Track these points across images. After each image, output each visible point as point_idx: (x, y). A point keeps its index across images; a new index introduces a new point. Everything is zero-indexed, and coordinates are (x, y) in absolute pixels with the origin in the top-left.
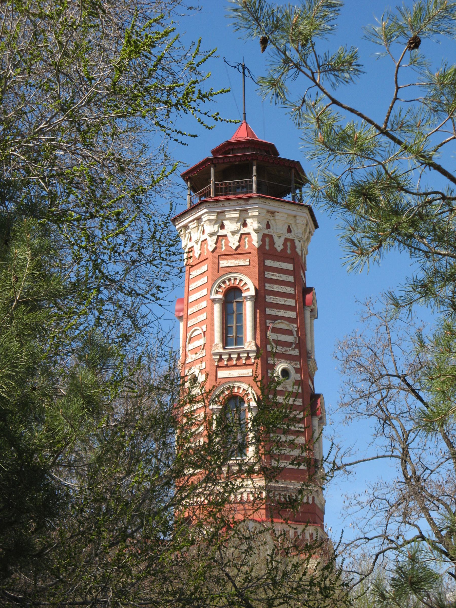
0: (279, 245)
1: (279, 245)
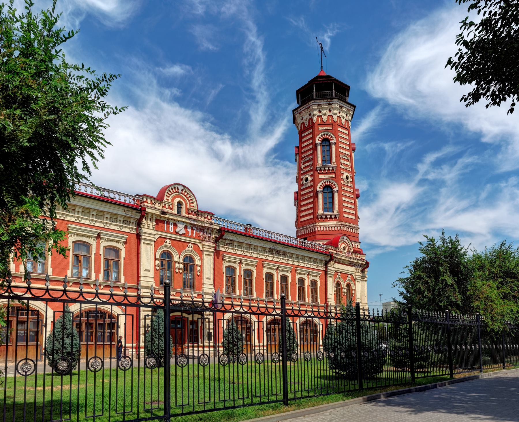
1: (343, 121)
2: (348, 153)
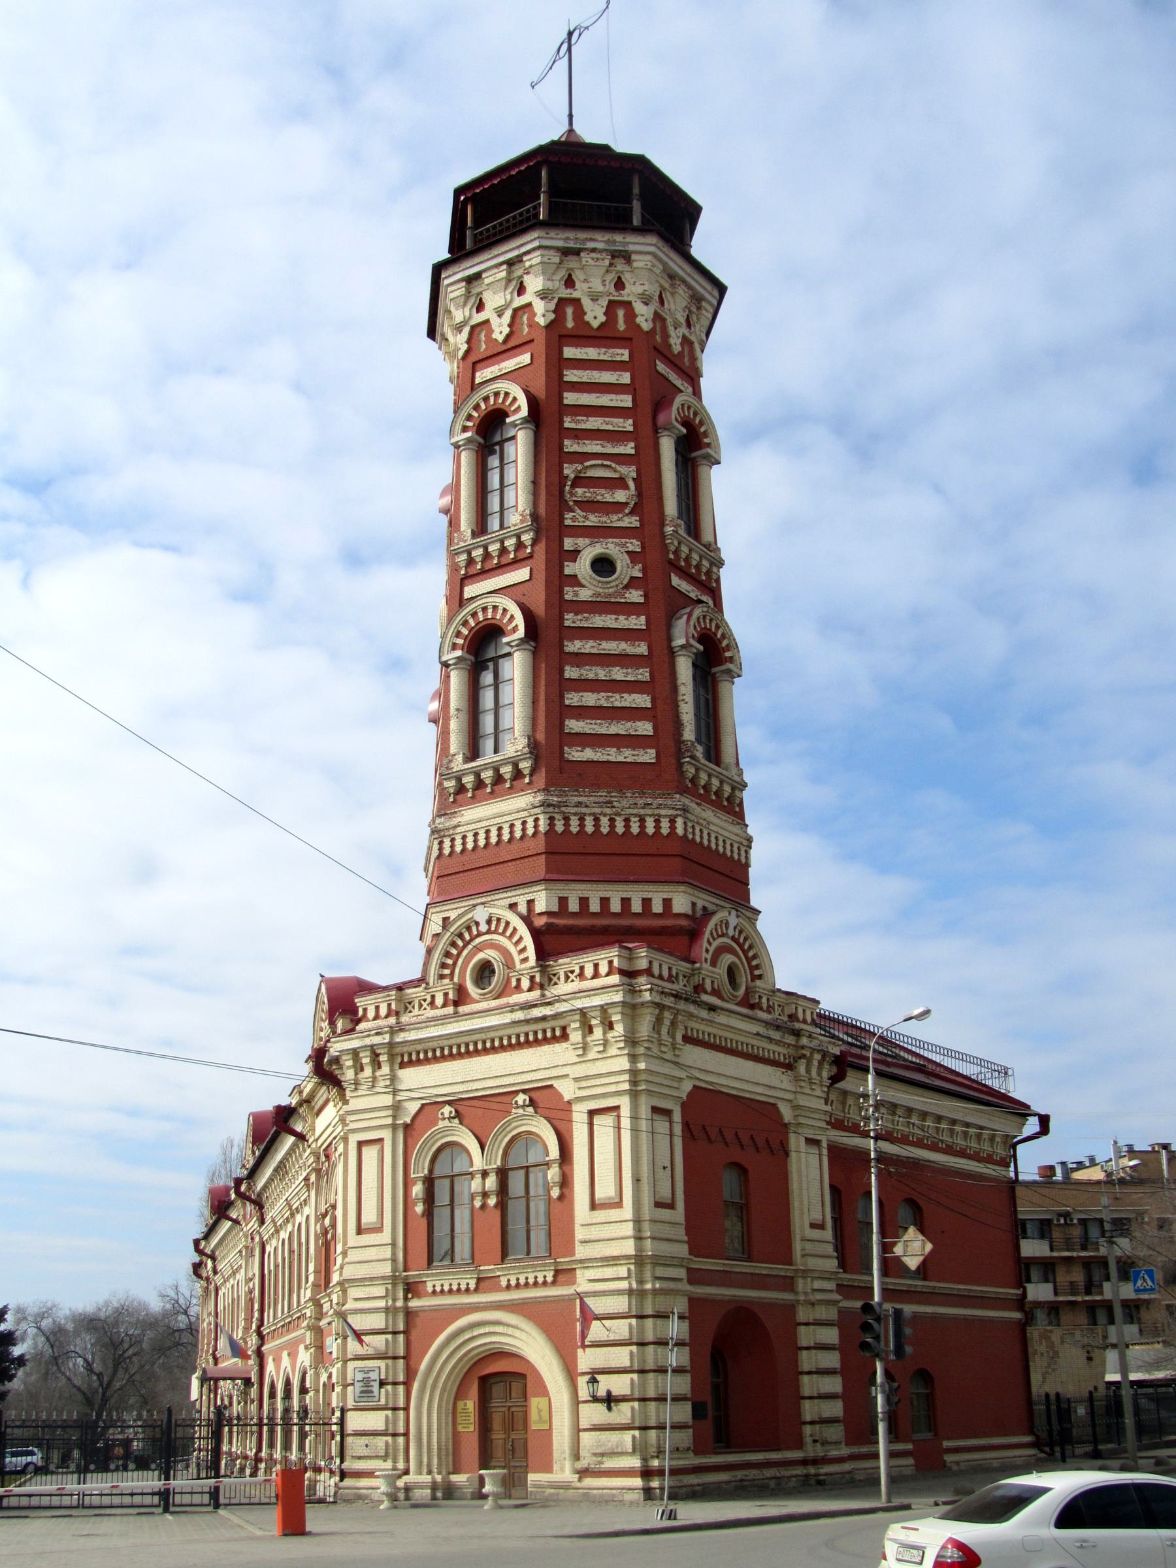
0: (595, 315)
1: (595, 315)
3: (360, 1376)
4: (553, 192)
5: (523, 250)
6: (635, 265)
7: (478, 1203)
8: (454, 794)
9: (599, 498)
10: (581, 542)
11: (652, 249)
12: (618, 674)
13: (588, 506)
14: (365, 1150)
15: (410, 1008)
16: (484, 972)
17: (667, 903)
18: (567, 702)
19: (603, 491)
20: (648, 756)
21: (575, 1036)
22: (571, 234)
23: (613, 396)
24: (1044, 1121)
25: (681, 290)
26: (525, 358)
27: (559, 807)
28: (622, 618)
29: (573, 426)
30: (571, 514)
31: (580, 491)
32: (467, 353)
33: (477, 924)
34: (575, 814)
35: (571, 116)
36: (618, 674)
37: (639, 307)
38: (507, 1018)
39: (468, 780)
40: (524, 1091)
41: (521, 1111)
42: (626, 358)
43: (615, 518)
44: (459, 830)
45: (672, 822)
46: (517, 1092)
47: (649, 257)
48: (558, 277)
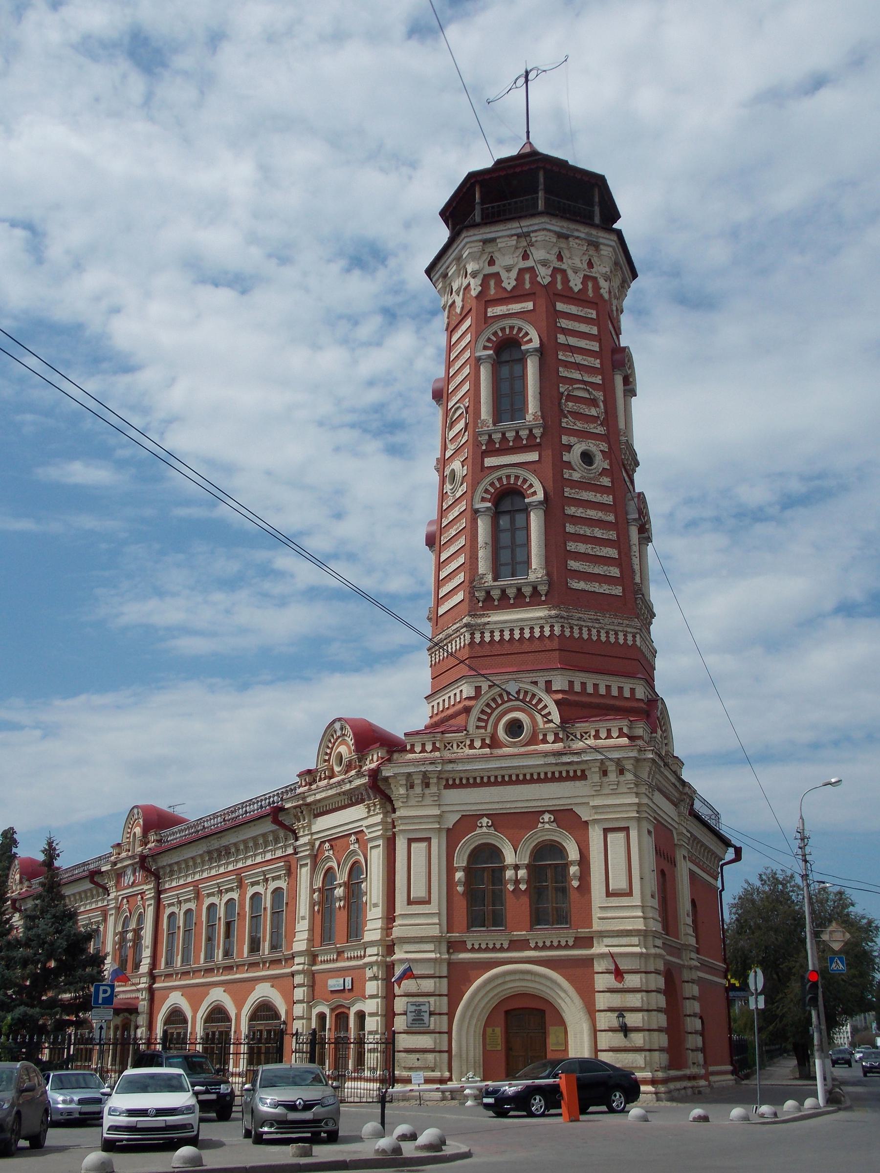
1: (576, 283)
2: (598, 380)
3: (413, 1008)
4: (547, 191)
5: (531, 229)
6: (602, 252)
7: (511, 887)
8: (483, 600)
9: (582, 411)
10: (573, 440)
11: (613, 244)
12: (598, 533)
13: (577, 415)
14: (413, 845)
15: (449, 747)
16: (515, 728)
17: (632, 691)
18: (568, 548)
19: (584, 407)
20: (618, 591)
21: (594, 777)
22: (565, 224)
23: (588, 342)
24: (738, 851)
25: (619, 273)
26: (529, 306)
27: (568, 619)
28: (598, 495)
29: (563, 358)
30: (566, 420)
31: (570, 404)
32: (480, 292)
33: (508, 693)
34: (577, 625)
35: (528, 132)
36: (598, 533)
37: (603, 283)
38: (541, 761)
39: (495, 594)
40: (549, 812)
41: (547, 826)
42: (594, 316)
43: (592, 426)
44: (487, 627)
45: (634, 637)
46: (543, 812)
47: (611, 249)
48: (553, 252)
